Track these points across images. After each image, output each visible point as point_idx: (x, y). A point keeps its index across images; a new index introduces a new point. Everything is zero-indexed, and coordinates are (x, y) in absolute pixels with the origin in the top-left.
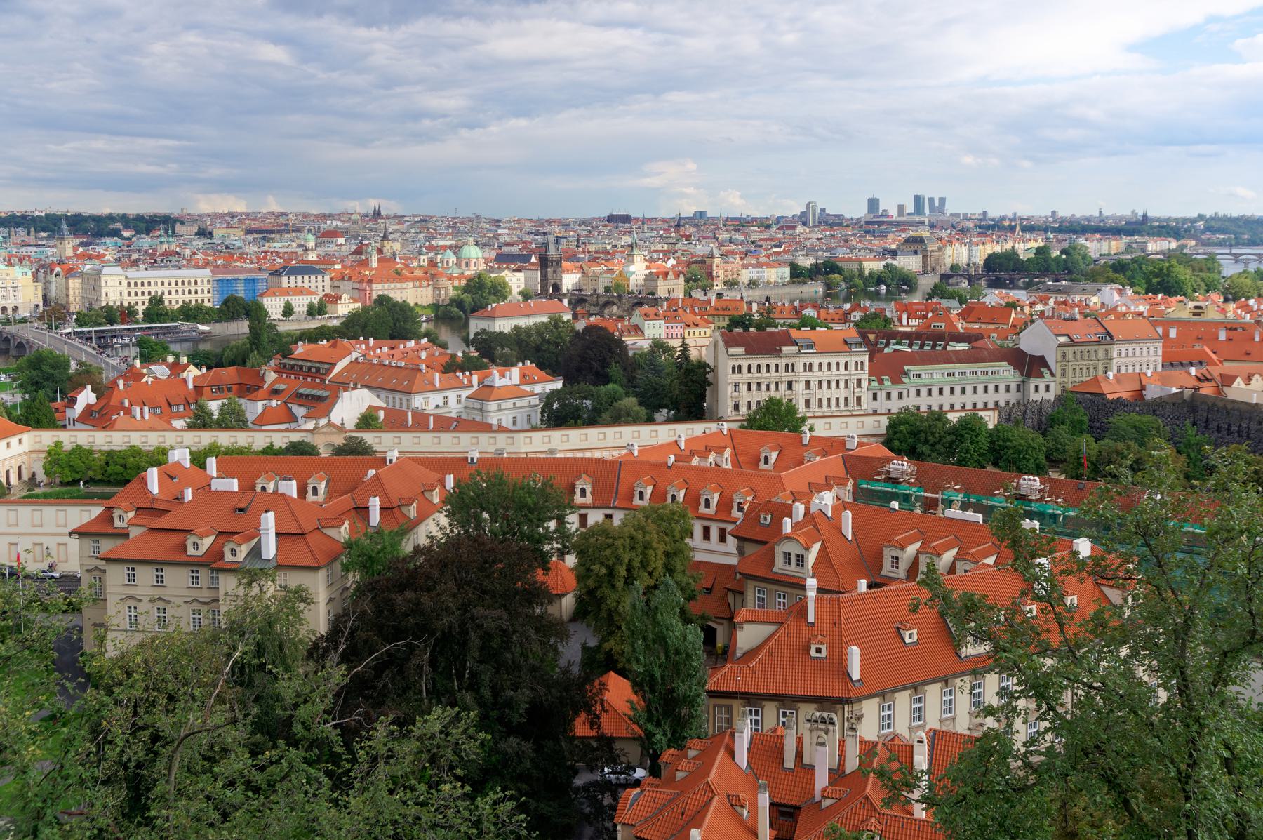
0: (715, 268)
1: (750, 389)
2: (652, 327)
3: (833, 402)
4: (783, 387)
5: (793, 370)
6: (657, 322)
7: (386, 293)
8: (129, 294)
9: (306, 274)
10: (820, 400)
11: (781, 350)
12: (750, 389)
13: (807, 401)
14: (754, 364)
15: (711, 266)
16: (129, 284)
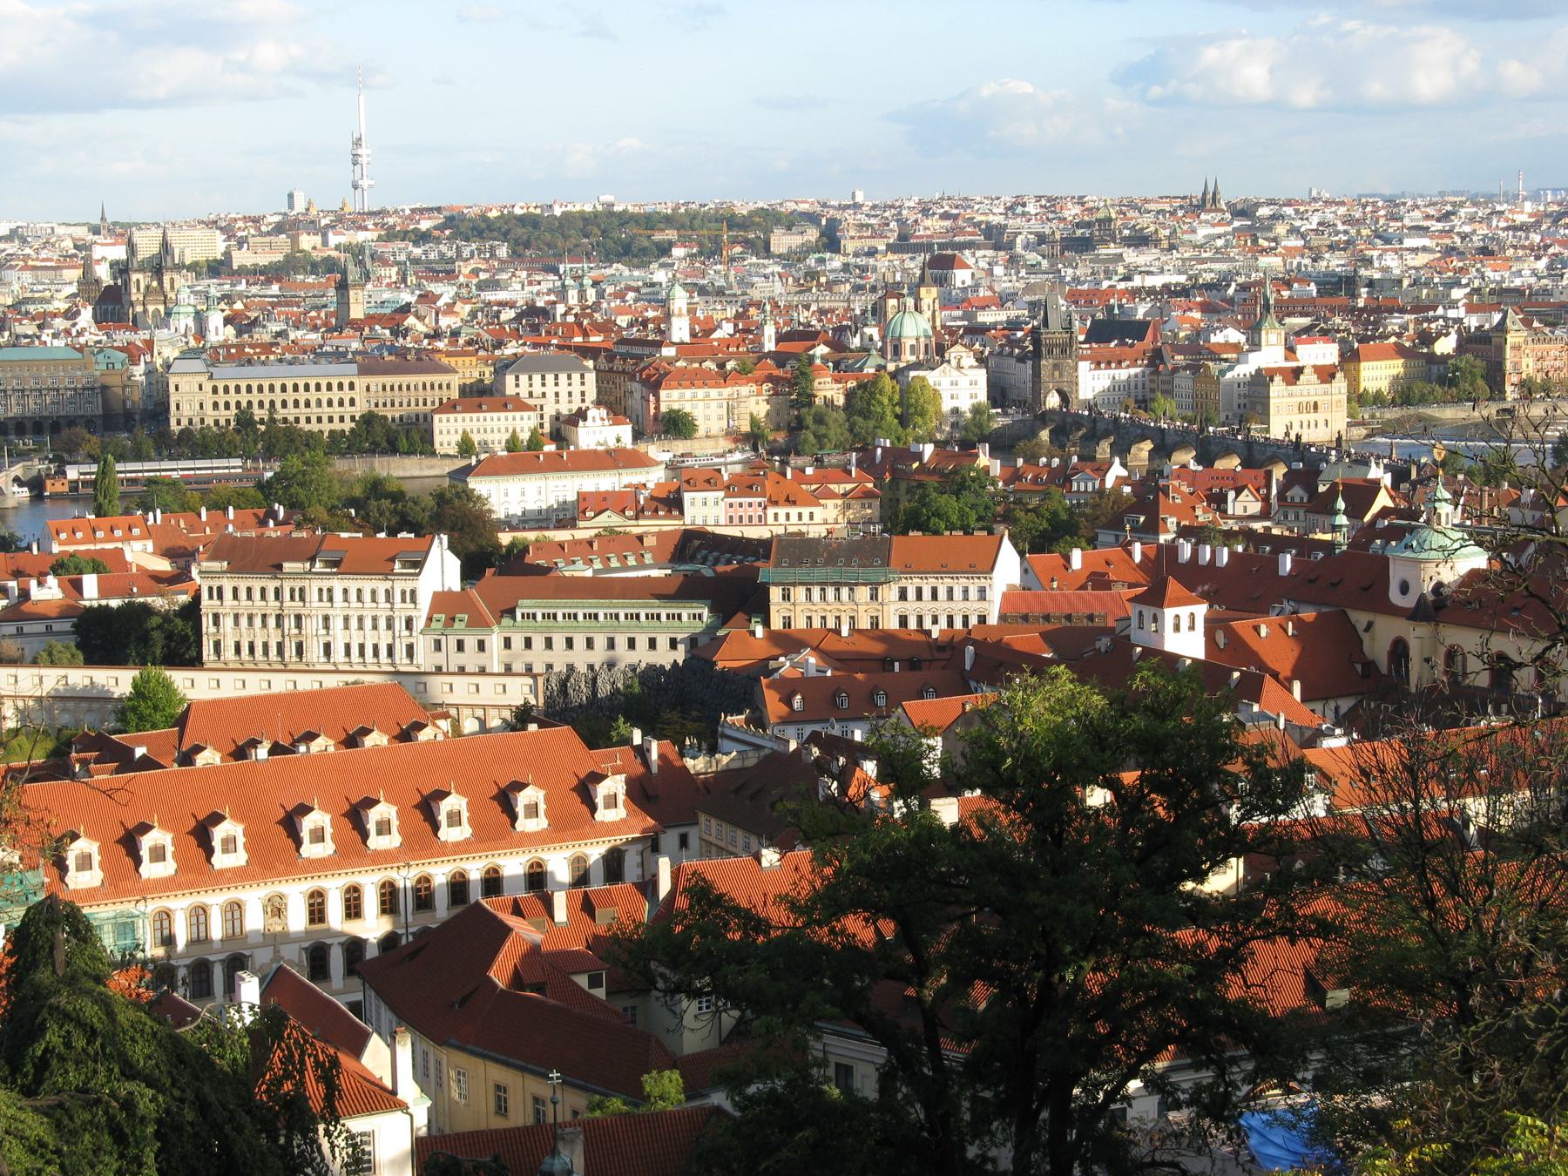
0: (1509, 353)
1: (237, 623)
2: (699, 502)
3: (369, 651)
4: (289, 623)
5: (302, 599)
6: (711, 496)
7: (687, 408)
8: (216, 405)
9: (562, 370)
10: (348, 647)
11: (280, 567)
12: (237, 623)
13: (327, 648)
14: (243, 586)
15: (1501, 350)
16: (215, 390)
